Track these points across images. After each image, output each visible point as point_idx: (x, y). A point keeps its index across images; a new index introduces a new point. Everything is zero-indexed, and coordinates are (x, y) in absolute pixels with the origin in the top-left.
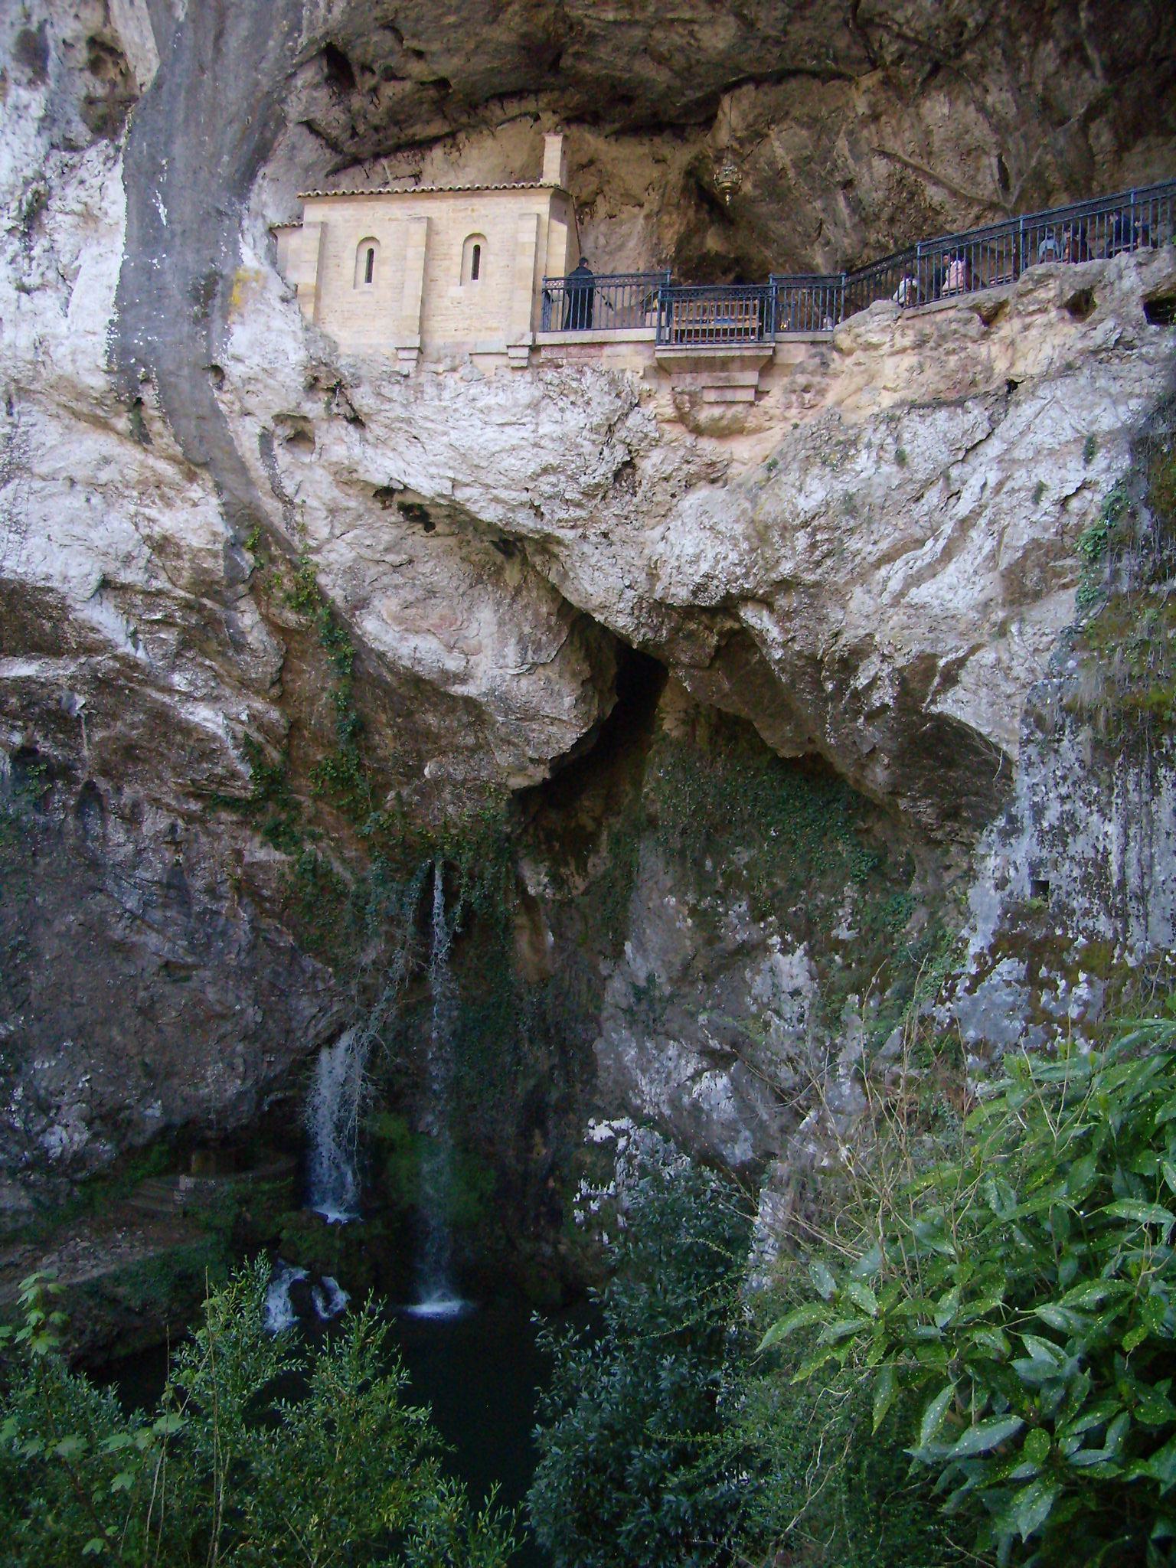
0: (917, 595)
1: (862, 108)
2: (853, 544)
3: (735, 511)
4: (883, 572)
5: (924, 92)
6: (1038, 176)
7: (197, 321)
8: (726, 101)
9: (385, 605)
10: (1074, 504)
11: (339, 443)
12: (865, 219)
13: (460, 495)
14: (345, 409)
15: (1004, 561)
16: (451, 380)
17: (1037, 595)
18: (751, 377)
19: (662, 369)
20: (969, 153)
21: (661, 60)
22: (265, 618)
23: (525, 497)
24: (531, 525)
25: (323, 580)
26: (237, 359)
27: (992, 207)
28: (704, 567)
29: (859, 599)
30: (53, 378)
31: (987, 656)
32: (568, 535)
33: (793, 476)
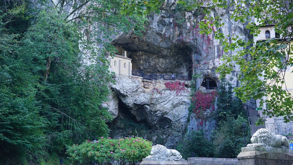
0: (165, 106)
1: (155, 57)
2: (159, 101)
10: (180, 100)
13: (120, 90)
15: (174, 104)
18: (150, 84)
20: (163, 64)
23: (126, 91)
24: (126, 94)
32: (129, 95)
33: (155, 94)
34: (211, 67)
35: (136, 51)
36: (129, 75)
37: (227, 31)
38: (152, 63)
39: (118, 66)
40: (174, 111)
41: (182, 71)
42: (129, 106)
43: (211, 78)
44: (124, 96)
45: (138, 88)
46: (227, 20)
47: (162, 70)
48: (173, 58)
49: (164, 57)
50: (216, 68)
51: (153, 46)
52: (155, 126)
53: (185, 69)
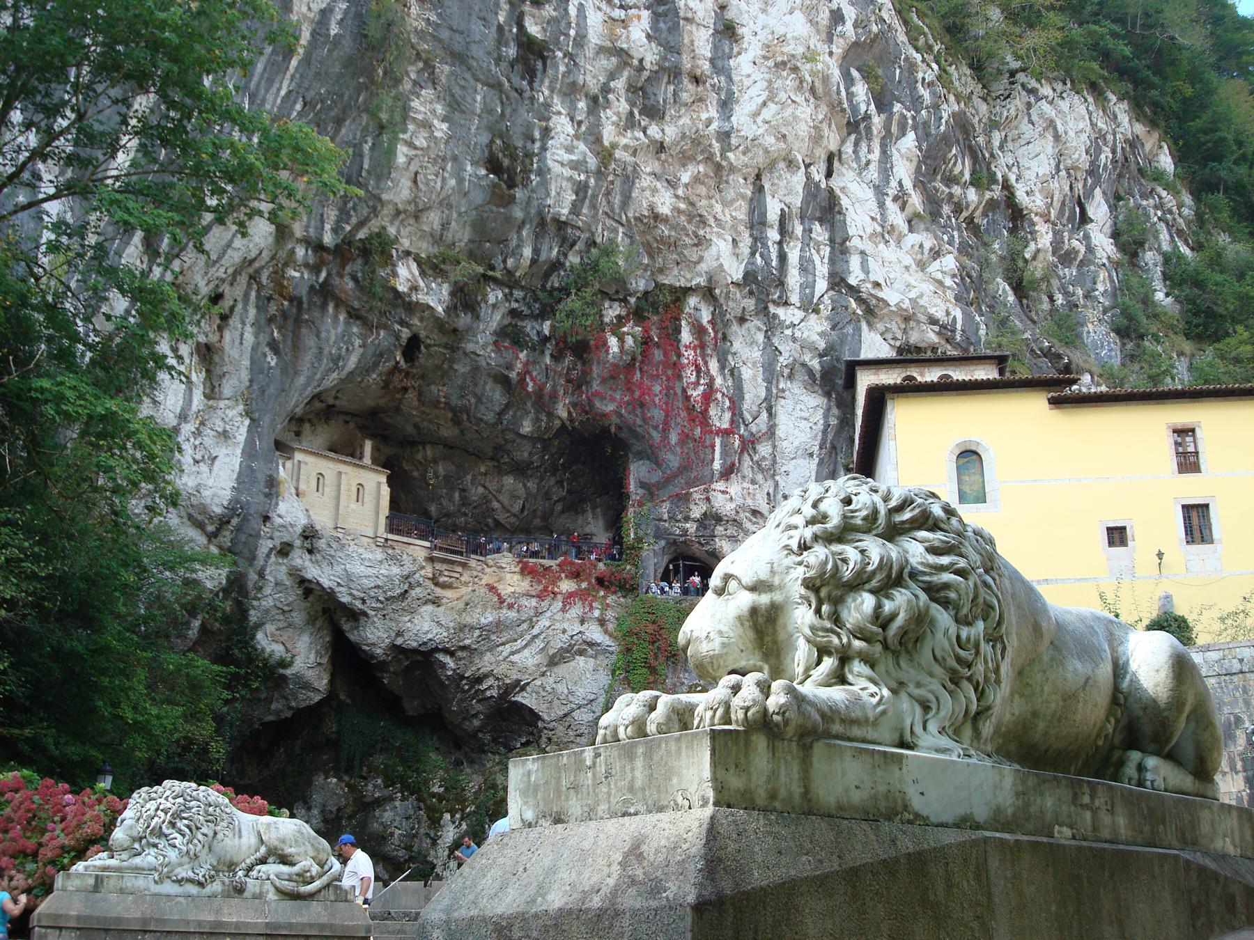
1: (483, 470)
2: (493, 637)
3: (450, 618)
4: (500, 648)
5: (507, 474)
6: (535, 511)
7: (268, 496)
8: (428, 448)
9: (270, 628)
11: (299, 559)
12: (465, 501)
13: (337, 589)
14: (309, 546)
15: (551, 652)
16: (352, 543)
17: (556, 664)
18: (459, 569)
19: (431, 559)
20: (514, 497)
21: (416, 426)
22: (203, 626)
24: (360, 606)
25: (252, 612)
26: (280, 516)
27: (515, 515)
28: (430, 636)
29: (488, 657)
30: (196, 503)
31: (538, 682)
34: (696, 512)
35: (412, 443)
36: (375, 533)
37: (760, 380)
38: (476, 492)
39: (333, 494)
40: (549, 681)
41: (587, 530)
42: (373, 657)
43: (698, 554)
44: (355, 616)
45: (411, 587)
46: (760, 337)
47: (513, 520)
48: (554, 474)
49: (520, 470)
50: (718, 519)
51: (477, 425)
52: (474, 736)
53: (601, 523)
